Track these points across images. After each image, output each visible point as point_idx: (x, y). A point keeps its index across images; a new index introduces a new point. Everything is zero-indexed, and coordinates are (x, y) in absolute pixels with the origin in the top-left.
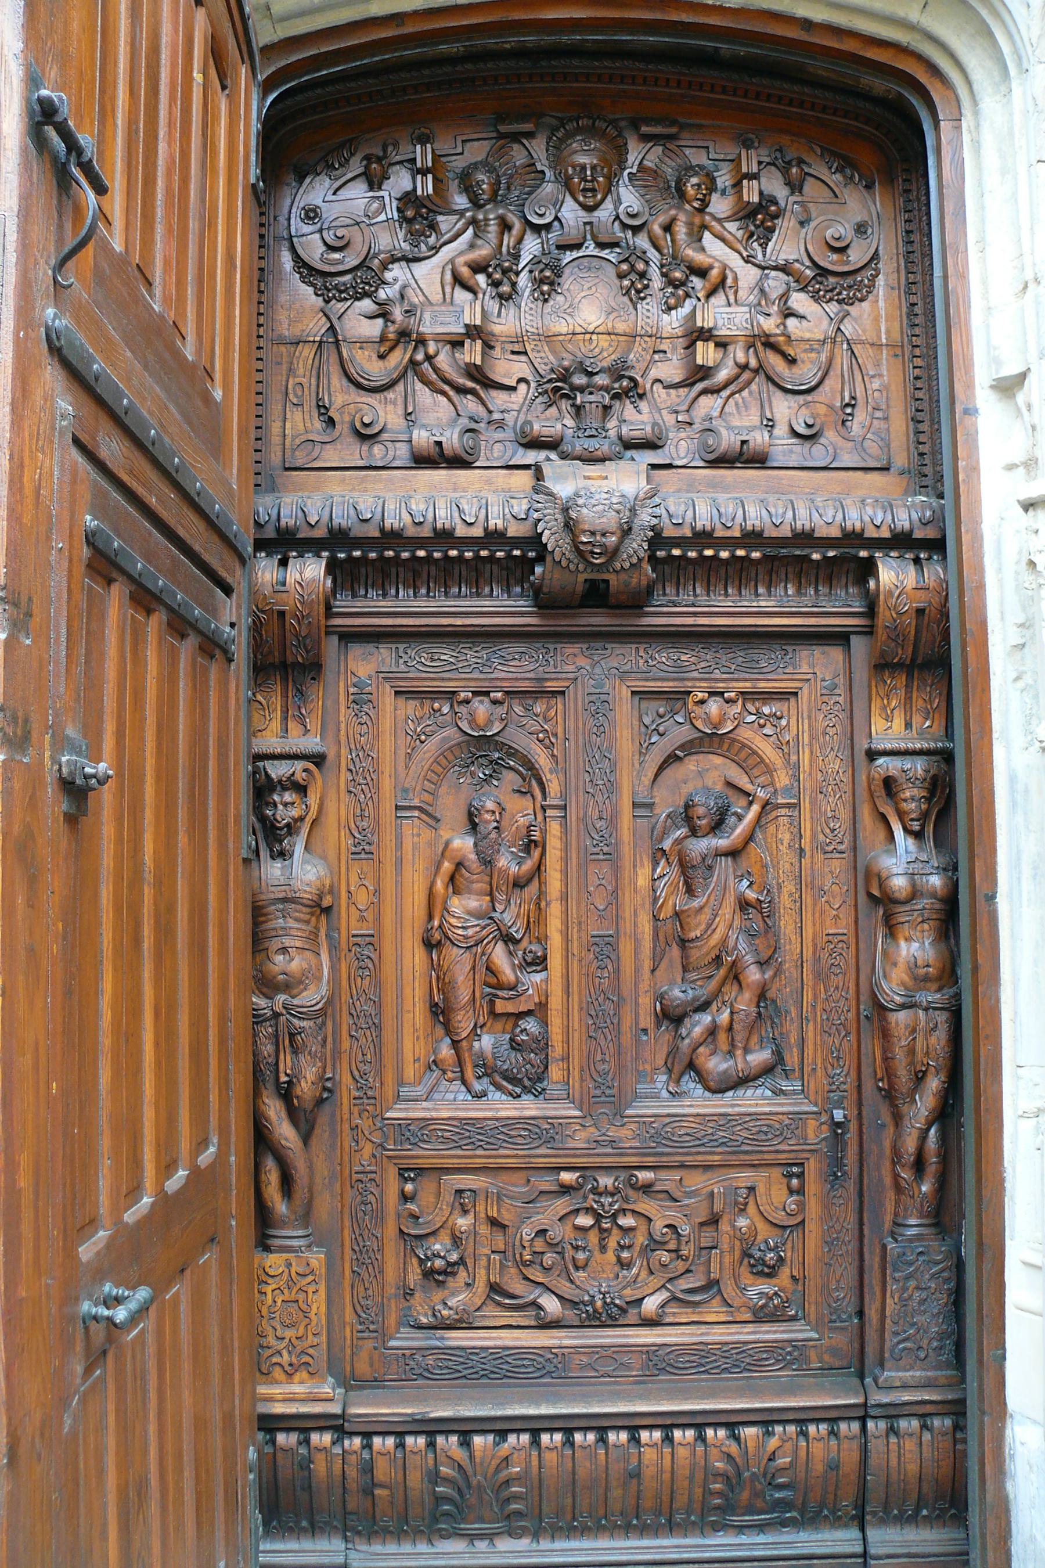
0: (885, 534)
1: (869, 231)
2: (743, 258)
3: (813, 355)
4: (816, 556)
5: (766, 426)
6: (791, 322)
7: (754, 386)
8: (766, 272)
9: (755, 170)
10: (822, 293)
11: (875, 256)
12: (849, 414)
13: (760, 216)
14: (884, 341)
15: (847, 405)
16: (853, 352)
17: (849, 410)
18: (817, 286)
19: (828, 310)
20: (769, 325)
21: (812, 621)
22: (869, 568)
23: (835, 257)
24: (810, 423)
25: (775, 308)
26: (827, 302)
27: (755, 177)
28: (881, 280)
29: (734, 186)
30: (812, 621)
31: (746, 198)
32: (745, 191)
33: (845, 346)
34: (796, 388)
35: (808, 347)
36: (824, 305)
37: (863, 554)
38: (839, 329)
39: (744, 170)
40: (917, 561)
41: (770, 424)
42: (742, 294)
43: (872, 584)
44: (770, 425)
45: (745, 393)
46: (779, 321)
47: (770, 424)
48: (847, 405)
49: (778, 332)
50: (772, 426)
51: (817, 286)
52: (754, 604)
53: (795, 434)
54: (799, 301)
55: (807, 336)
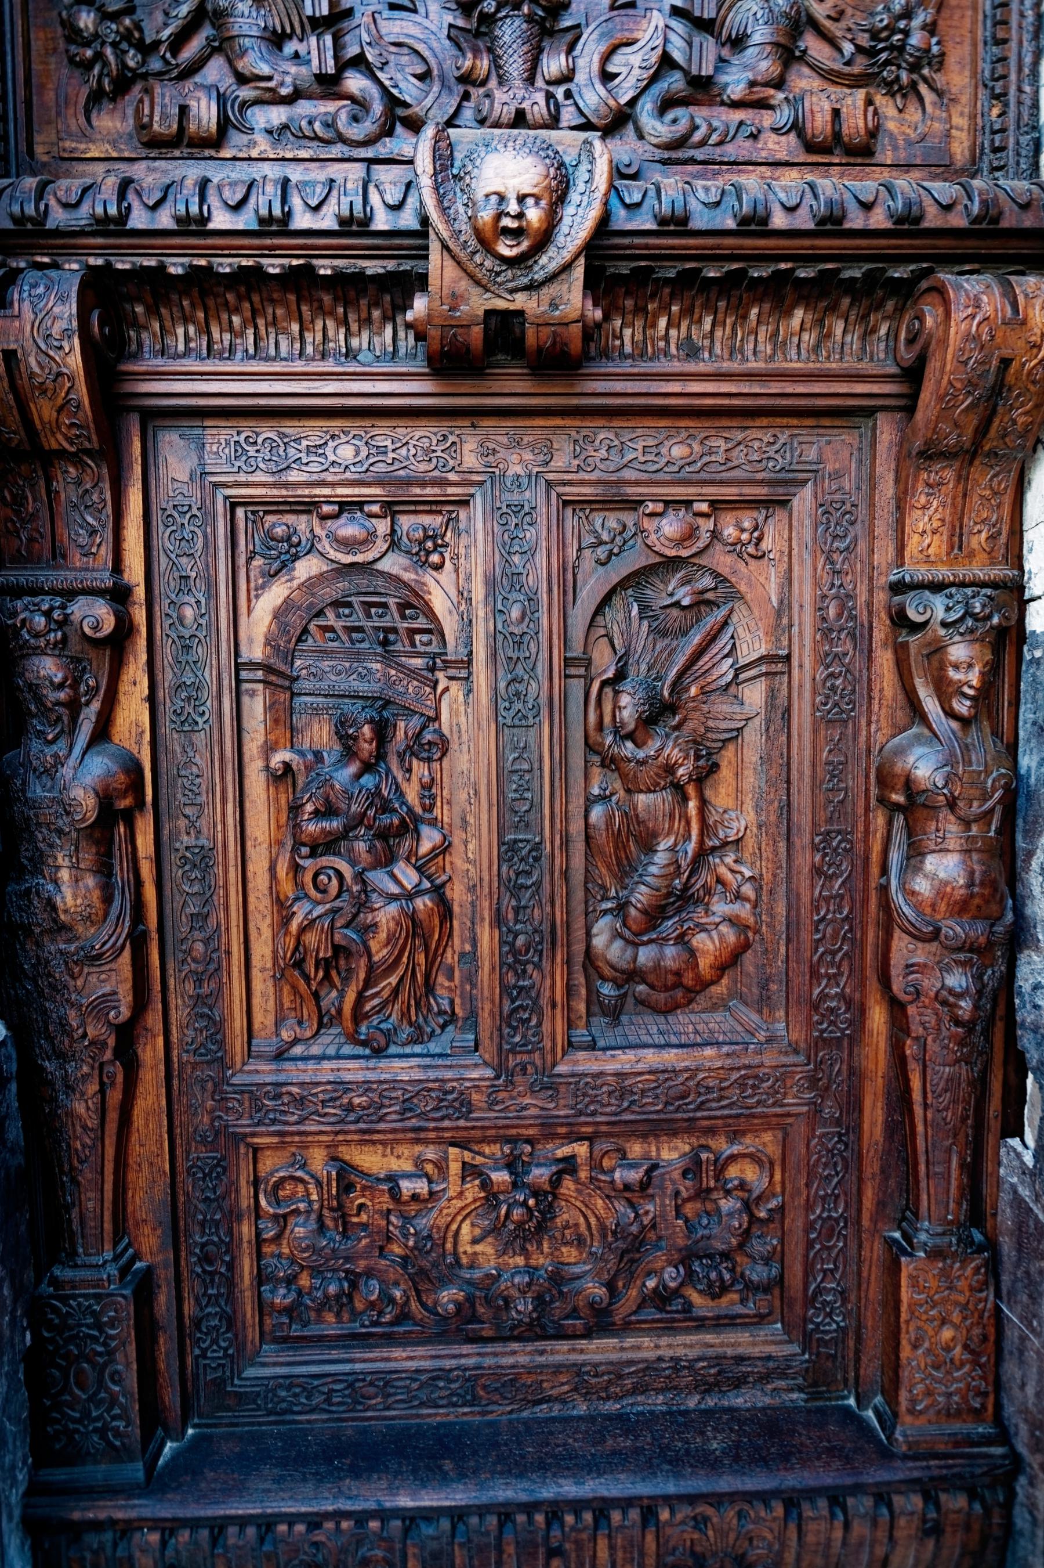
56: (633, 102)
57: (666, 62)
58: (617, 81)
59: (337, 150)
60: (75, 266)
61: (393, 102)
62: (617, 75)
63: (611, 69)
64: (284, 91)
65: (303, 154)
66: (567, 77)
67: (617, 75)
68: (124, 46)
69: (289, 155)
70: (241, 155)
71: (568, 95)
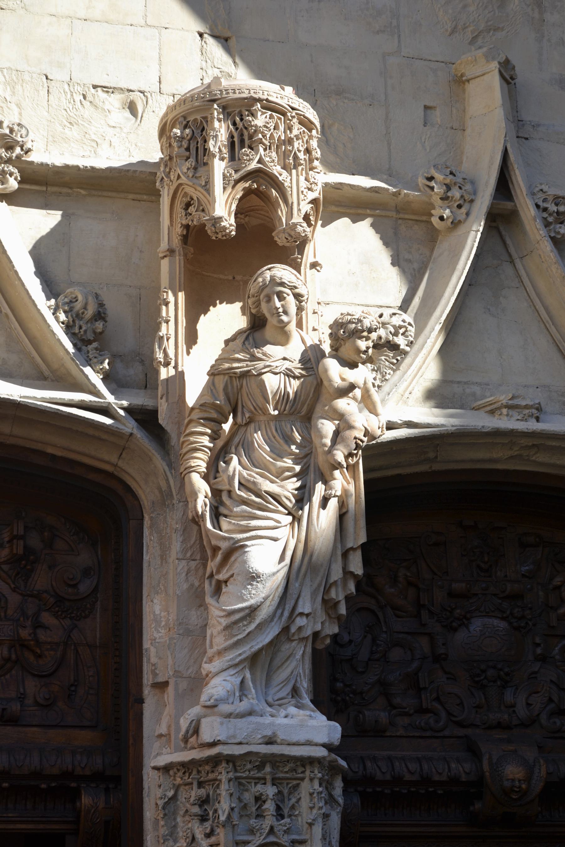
0: (88, 772)
1: (92, 573)
2: (11, 588)
3: (52, 653)
4: (43, 786)
5: (20, 698)
6: (40, 632)
7: (13, 672)
8: (26, 598)
9: (21, 532)
10: (60, 613)
11: (95, 590)
12: (73, 691)
13: (23, 562)
14: (98, 644)
15: (72, 685)
16: (77, 651)
17: (73, 688)
18: (57, 609)
19: (64, 624)
20: (25, 634)
21: (41, 826)
22: (75, 795)
23: (70, 590)
24: (47, 697)
25: (30, 623)
26: (63, 619)
27: (22, 537)
28: (98, 605)
29: (9, 542)
30: (41, 826)
31: (15, 552)
32: (15, 547)
33: (73, 647)
34: (40, 674)
35: (49, 647)
36: (61, 620)
37: (73, 785)
38: (69, 636)
39: (15, 533)
40: (107, 790)
41: (22, 696)
42: (10, 612)
43: (78, 804)
44: (22, 697)
45: (8, 676)
46: (31, 631)
47: (22, 696)
48: (72, 685)
49: (30, 638)
50: (23, 698)
51: (57, 609)
52: (5, 815)
53: (37, 703)
54: (47, 618)
55: (49, 640)
56: (539, 715)
57: (551, 700)
58: (533, 706)
59: (428, 734)
60: (352, 790)
61: (449, 714)
62: (531, 705)
63: (529, 702)
64: (412, 712)
65: (417, 734)
66: (513, 706)
67: (531, 705)
68: (351, 695)
69: (411, 735)
70: (393, 735)
71: (514, 711)
